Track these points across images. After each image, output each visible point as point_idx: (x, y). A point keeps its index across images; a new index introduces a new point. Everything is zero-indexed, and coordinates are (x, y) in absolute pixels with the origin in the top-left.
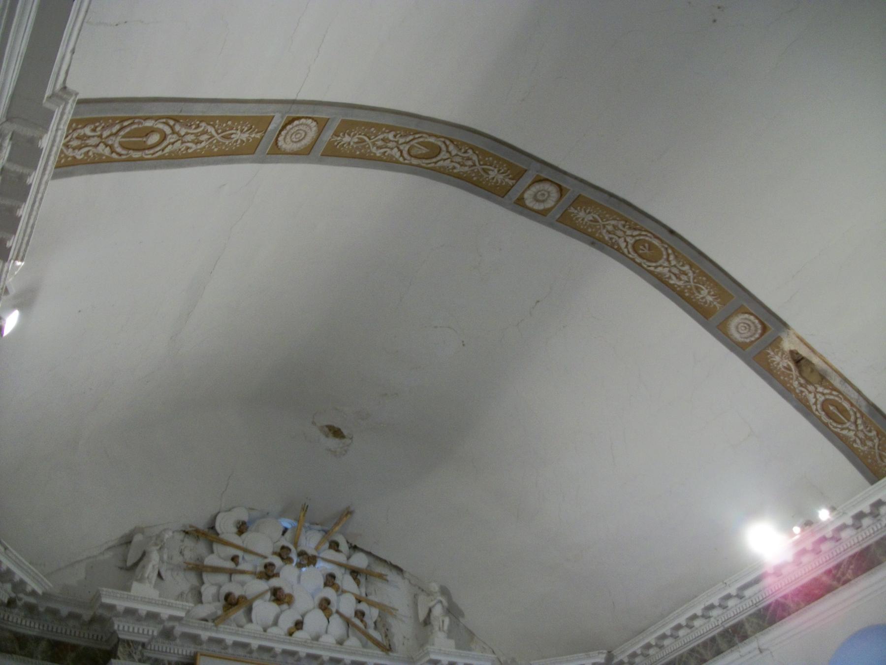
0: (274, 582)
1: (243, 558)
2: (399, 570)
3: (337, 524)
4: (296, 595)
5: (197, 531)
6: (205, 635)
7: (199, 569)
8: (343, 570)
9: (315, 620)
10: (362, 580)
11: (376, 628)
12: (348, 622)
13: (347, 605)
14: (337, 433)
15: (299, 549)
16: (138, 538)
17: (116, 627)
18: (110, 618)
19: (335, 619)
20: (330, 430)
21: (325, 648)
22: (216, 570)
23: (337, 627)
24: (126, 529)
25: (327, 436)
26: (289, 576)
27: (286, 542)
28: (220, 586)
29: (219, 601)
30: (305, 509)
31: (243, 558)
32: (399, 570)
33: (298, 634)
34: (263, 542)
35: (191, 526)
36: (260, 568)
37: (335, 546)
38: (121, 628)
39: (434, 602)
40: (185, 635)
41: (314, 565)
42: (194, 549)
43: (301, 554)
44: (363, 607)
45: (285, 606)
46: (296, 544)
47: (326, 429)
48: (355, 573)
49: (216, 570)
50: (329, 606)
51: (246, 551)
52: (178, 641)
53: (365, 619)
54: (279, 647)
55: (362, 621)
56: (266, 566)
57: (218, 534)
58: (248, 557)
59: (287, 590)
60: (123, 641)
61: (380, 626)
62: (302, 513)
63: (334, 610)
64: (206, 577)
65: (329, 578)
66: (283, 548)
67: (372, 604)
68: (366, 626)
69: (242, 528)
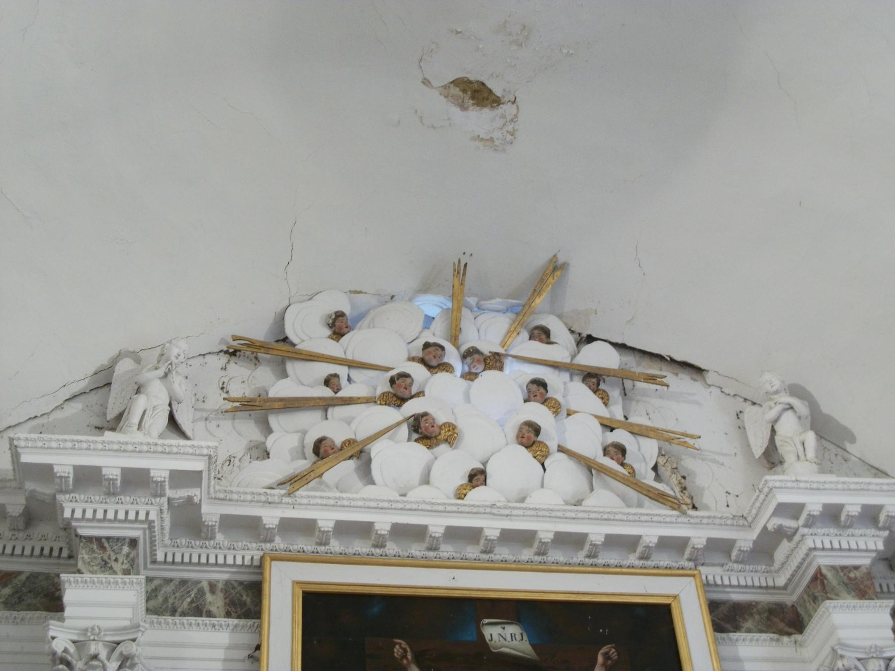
0: (412, 407)
1: (349, 379)
2: (696, 370)
3: (536, 292)
4: (460, 424)
5: (252, 344)
6: (271, 517)
7: (259, 408)
8: (566, 376)
9: (512, 467)
10: (615, 394)
11: (658, 478)
12: (590, 467)
13: (586, 437)
14: (478, 94)
15: (464, 348)
16: (125, 366)
17: (67, 514)
18: (54, 497)
19: (556, 461)
20: (464, 91)
21: (538, 513)
22: (291, 405)
23: (563, 476)
24: (103, 360)
25: (463, 108)
26: (440, 395)
27: (436, 335)
28: (304, 433)
29: (305, 458)
30: (461, 271)
31: (349, 379)
32: (696, 370)
33: (477, 495)
34: (386, 343)
35: (235, 338)
36: (383, 386)
37: (543, 334)
38: (78, 514)
39: (779, 408)
40: (230, 523)
41: (501, 369)
42: (246, 380)
43: (470, 354)
44: (620, 436)
45: (443, 447)
46: (454, 339)
47: (456, 91)
48: (593, 378)
49: (291, 405)
50: (540, 438)
51: (352, 365)
52: (219, 537)
53: (628, 460)
54: (437, 525)
55: (622, 464)
56: (392, 381)
57: (294, 345)
58: (355, 374)
59: (441, 418)
60: (90, 539)
61: (665, 471)
62: (458, 281)
63: (553, 446)
64: (273, 420)
65: (534, 387)
66: (427, 345)
67: (638, 432)
68: (633, 473)
69: (338, 326)
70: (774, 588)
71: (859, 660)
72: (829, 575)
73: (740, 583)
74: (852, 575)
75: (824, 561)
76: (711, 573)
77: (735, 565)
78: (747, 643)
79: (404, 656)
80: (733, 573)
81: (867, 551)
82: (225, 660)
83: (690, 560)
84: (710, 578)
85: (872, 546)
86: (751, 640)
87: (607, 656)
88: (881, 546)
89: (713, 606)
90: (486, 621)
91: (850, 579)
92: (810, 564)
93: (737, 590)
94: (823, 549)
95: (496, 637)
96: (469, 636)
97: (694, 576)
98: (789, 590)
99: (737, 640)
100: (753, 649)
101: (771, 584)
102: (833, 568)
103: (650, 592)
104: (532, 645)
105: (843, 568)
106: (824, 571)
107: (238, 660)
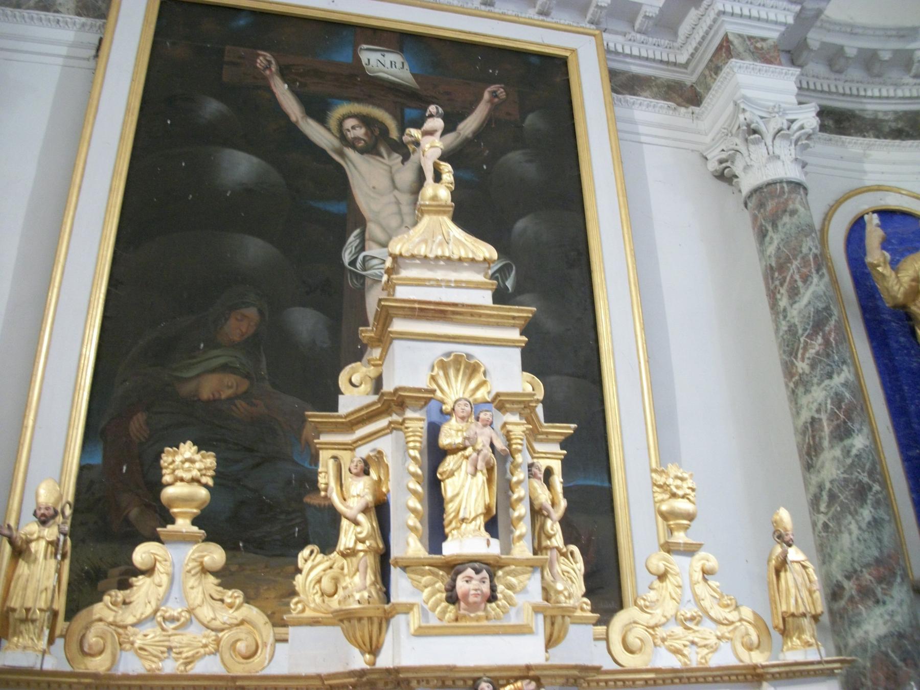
70: (675, 64)
71: (762, 118)
72: (736, 41)
73: (642, 52)
74: (759, 45)
75: (731, 27)
76: (614, 41)
77: (638, 36)
78: (644, 108)
79: (268, 67)
80: (635, 44)
81: (776, 23)
82: (67, 57)
83: (592, 23)
84: (612, 45)
85: (781, 19)
86: (648, 106)
87: (494, 94)
88: (790, 20)
89: (613, 74)
90: (365, 46)
91: (756, 48)
92: (719, 27)
93: (638, 62)
94: (732, 14)
95: (373, 62)
96: (343, 57)
97: (594, 35)
98: (692, 65)
99: (634, 104)
100: (647, 112)
101: (672, 59)
102: (740, 36)
103: (546, 42)
104: (414, 75)
105: (750, 38)
106: (731, 38)
107: (84, 59)
